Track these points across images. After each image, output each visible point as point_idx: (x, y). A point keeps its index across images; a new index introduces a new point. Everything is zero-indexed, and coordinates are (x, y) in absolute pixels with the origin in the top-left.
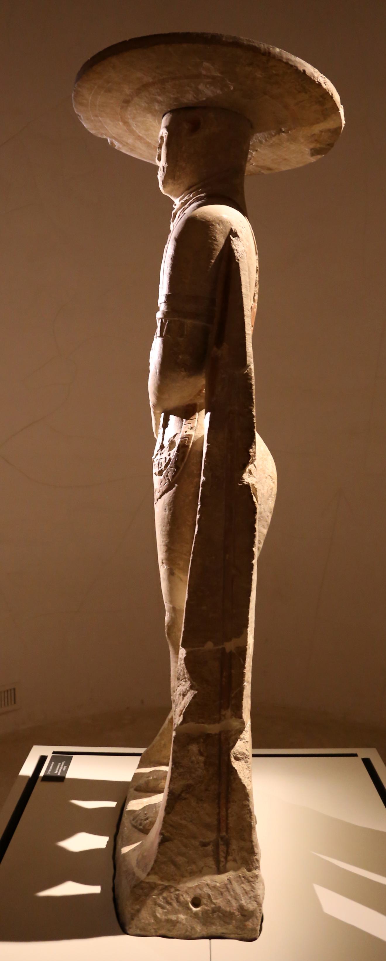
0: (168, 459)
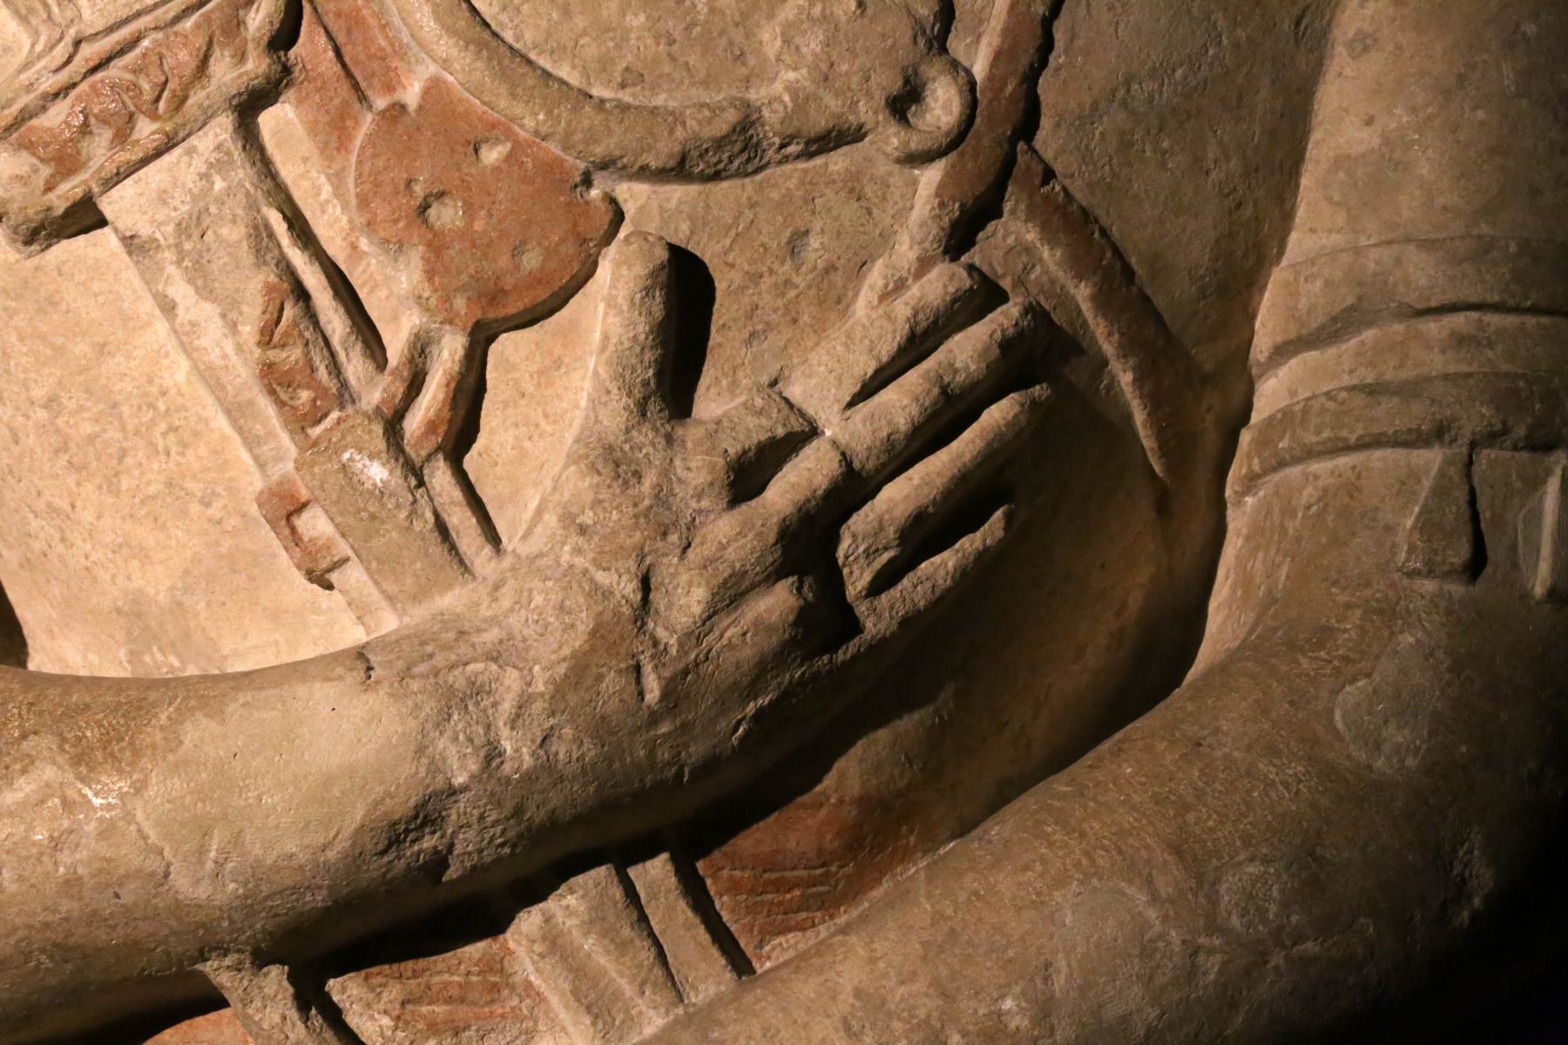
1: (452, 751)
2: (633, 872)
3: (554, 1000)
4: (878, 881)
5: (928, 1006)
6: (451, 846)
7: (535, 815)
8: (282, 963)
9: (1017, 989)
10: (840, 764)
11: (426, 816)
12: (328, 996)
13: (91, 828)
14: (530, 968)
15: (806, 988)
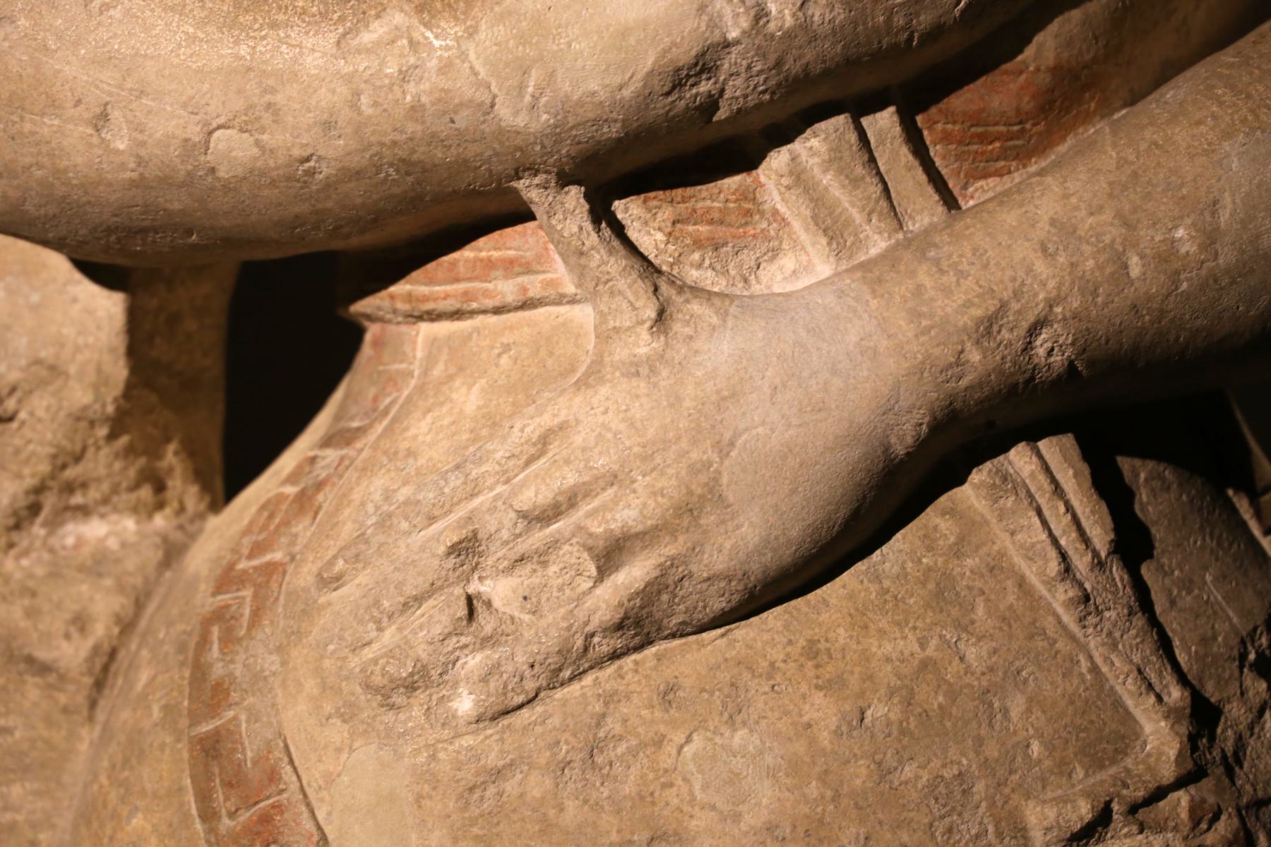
1: (728, 11)
2: (865, 121)
3: (796, 225)
4: (1063, 138)
5: (1114, 233)
6: (722, 91)
7: (792, 66)
8: (580, 184)
9: (1189, 221)
10: (1038, 39)
11: (704, 65)
12: (613, 215)
13: (433, 64)
14: (777, 198)
15: (1010, 217)
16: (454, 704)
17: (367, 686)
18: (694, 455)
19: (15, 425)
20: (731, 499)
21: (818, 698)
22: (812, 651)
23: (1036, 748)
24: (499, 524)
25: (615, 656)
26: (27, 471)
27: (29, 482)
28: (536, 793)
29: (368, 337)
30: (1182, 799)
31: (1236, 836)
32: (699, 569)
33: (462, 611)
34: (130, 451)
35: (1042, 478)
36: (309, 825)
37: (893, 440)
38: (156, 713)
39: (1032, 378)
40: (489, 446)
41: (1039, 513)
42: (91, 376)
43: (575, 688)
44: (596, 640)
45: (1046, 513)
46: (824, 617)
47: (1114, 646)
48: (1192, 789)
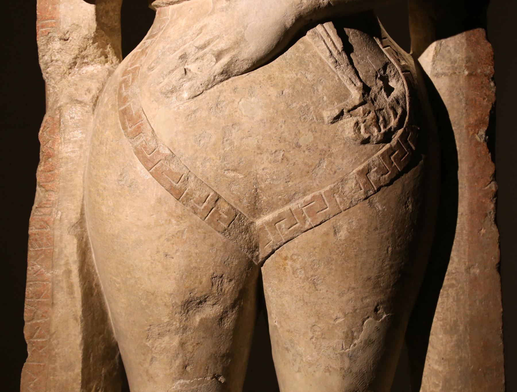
0: (399, 111)
16: (183, 95)
17: (161, 93)
18: (238, 30)
19: (68, 41)
20: (247, 39)
21: (272, 89)
22: (270, 78)
23: (325, 98)
24: (191, 51)
25: (221, 81)
26: (72, 53)
27: (73, 56)
28: (204, 115)
29: (157, 12)
30: (361, 109)
31: (374, 117)
32: (241, 58)
33: (184, 72)
34: (98, 47)
35: (325, 33)
36: (149, 128)
37: (286, 23)
38: (110, 107)
39: (319, 6)
40: (188, 32)
41: (324, 41)
42: (87, 27)
43: (212, 89)
44: (216, 77)
45: (326, 41)
46: (272, 69)
47: (344, 73)
48: (363, 106)
